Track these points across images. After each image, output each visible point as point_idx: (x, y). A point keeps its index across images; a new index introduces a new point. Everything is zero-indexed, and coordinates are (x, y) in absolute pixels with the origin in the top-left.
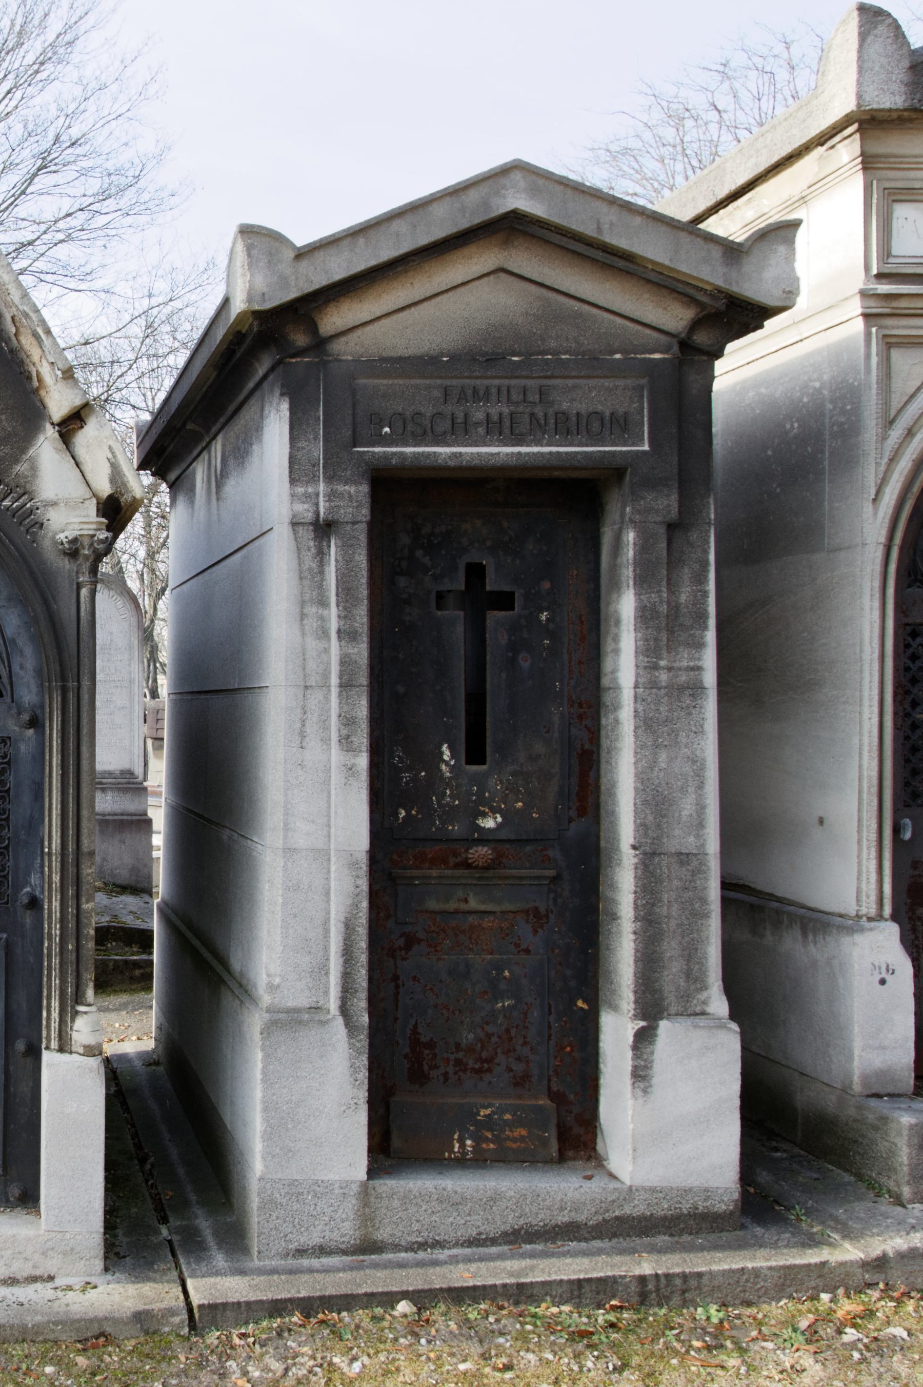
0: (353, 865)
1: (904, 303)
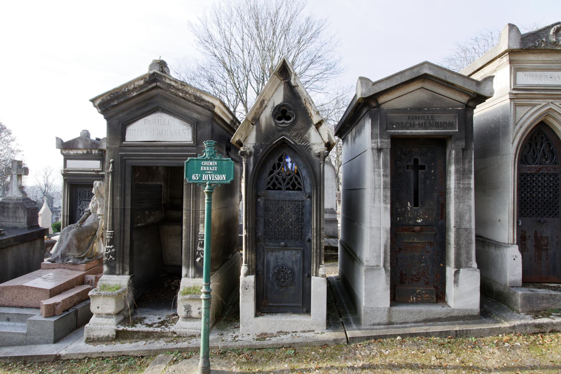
0: (387, 231)
1: (519, 96)
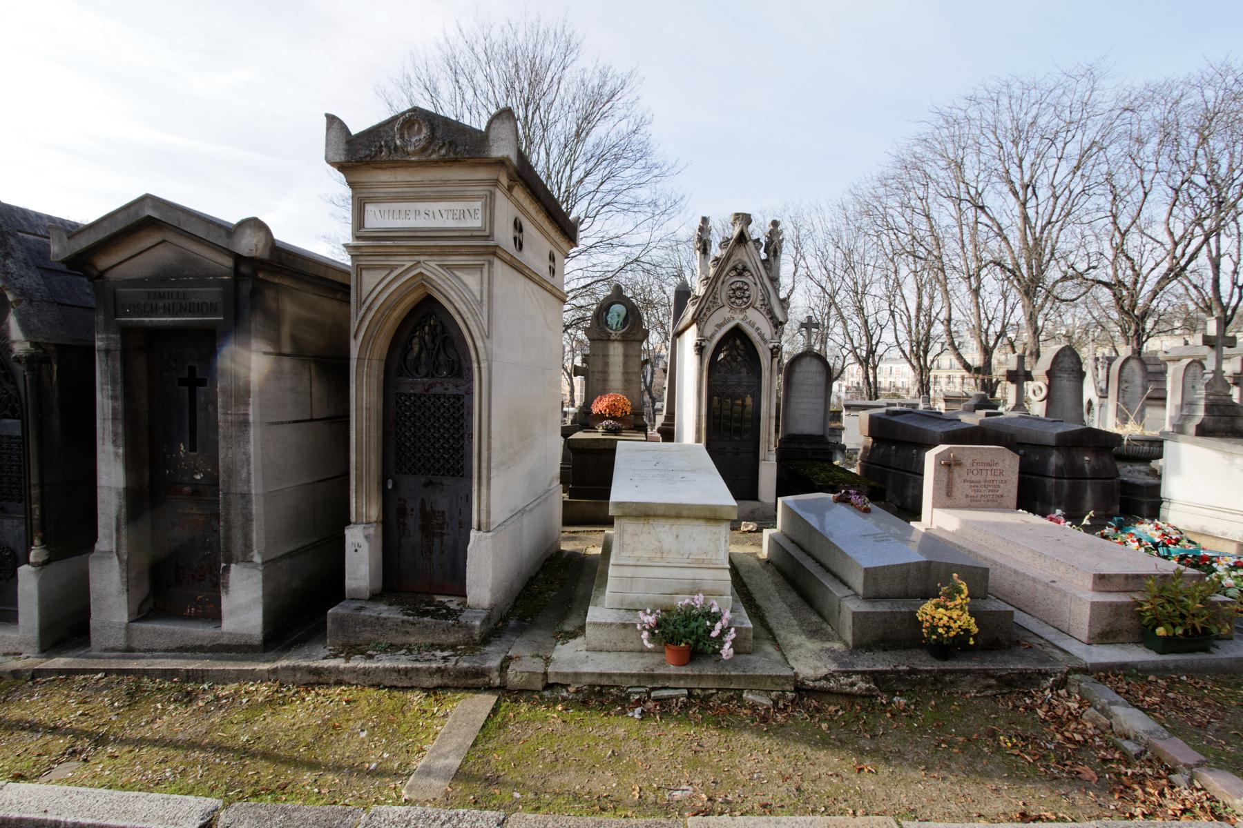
0: (118, 493)
1: (364, 250)
